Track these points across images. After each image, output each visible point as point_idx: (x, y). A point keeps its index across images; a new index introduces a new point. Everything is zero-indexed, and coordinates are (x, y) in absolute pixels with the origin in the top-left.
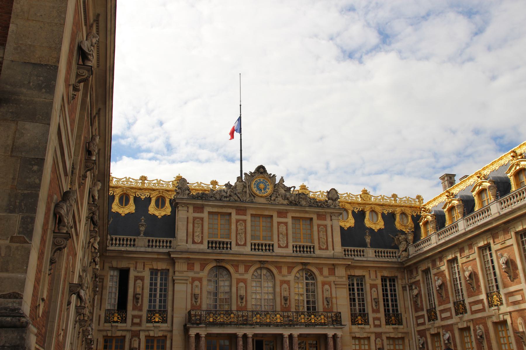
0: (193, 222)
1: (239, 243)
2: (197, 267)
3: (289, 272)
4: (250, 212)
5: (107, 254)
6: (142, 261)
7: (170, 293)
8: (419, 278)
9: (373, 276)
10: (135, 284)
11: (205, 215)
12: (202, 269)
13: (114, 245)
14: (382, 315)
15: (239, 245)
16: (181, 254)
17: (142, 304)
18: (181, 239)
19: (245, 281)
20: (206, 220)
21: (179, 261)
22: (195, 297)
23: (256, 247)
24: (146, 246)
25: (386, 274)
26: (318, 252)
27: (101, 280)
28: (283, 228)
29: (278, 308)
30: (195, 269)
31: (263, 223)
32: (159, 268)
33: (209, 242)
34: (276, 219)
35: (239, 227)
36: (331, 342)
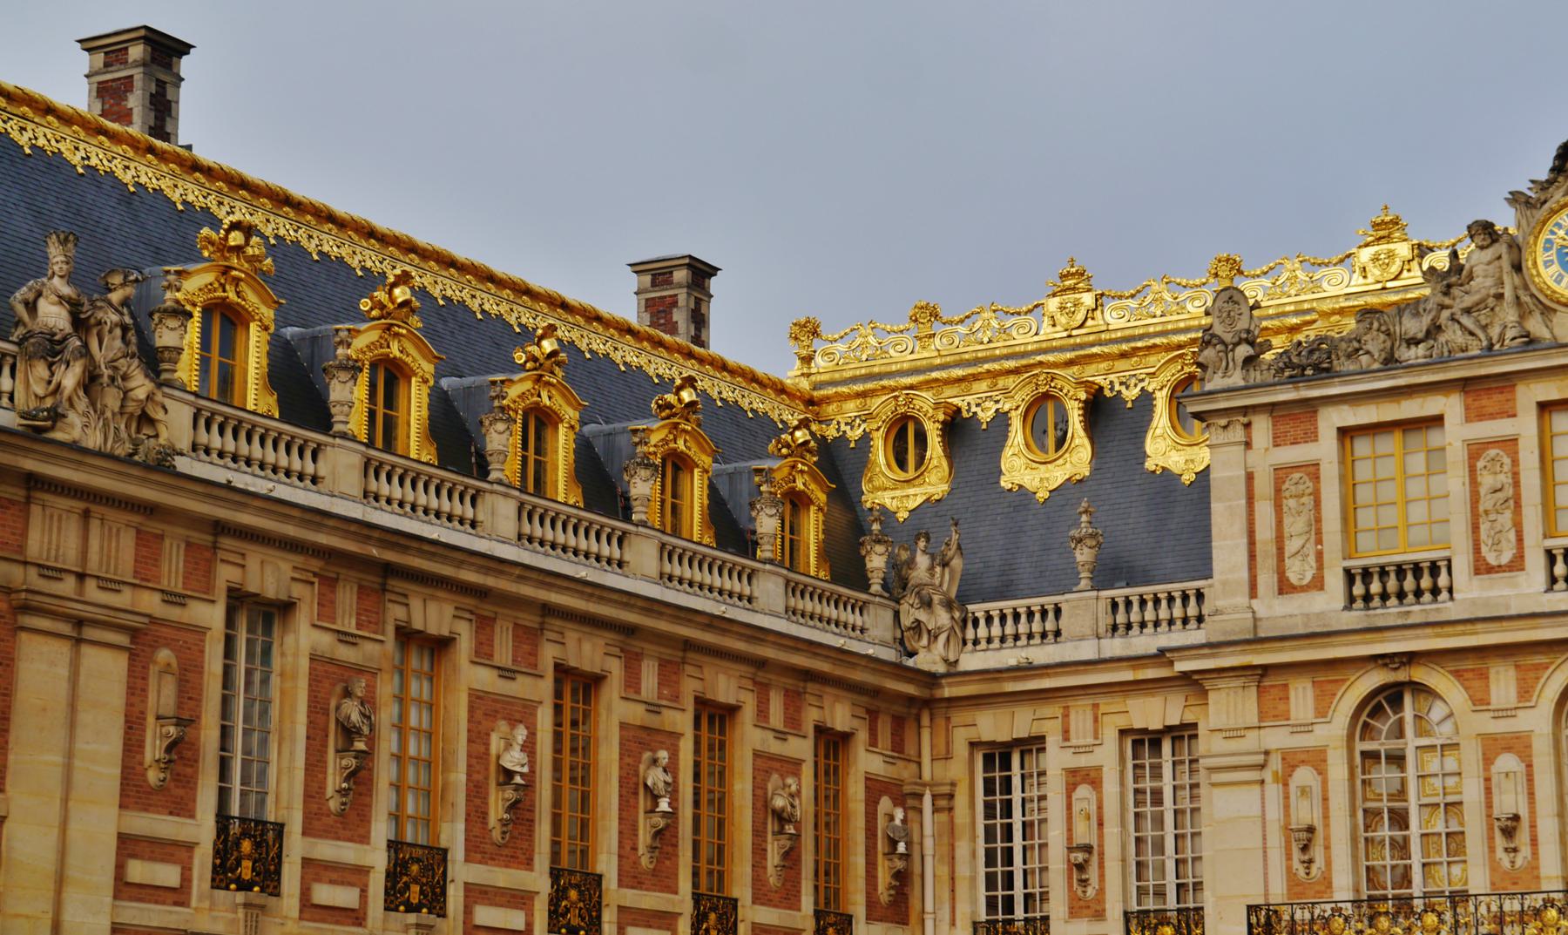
0: (1278, 491)
1: (1492, 561)
4: (1530, 394)
5: (947, 692)
6: (1090, 701)
10: (1069, 807)
13: (983, 645)
15: (1490, 570)
16: (1213, 656)
17: (1101, 891)
18: (1224, 583)
21: (1222, 684)
22: (1305, 840)
24: (1102, 630)
27: (943, 803)
30: (1293, 714)
32: (1156, 725)
33: (1349, 576)
35: (1487, 481)
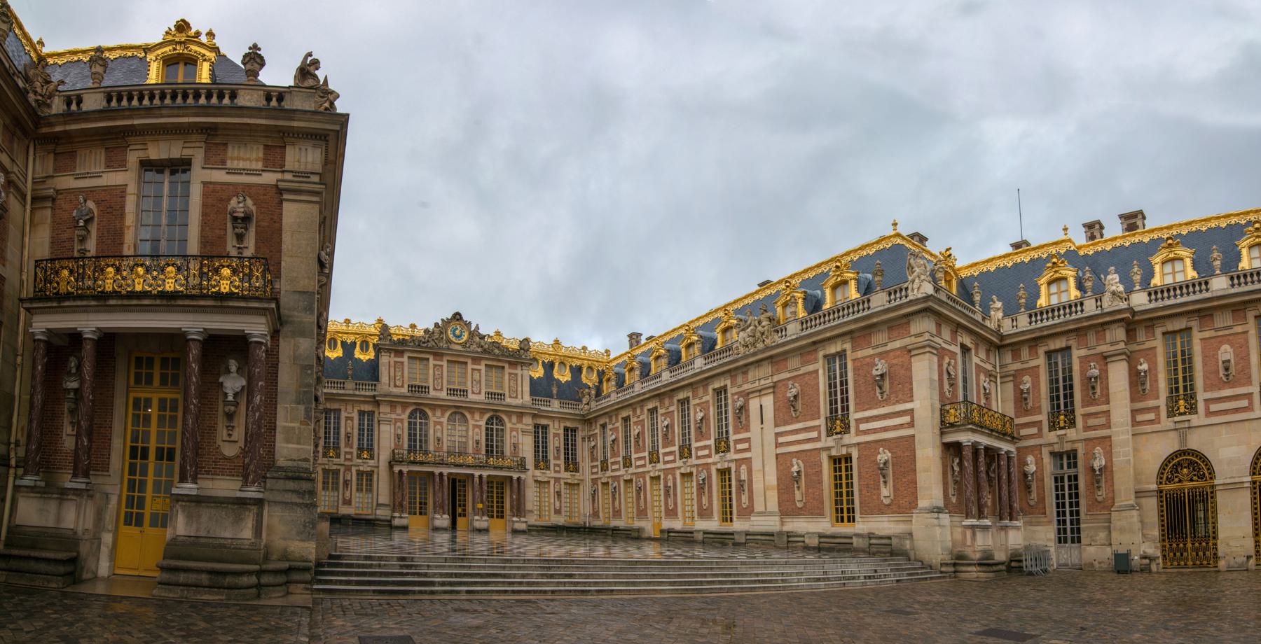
2: (399, 410)
3: (481, 418)
4: (445, 358)
7: (376, 433)
8: (597, 431)
9: (557, 426)
11: (405, 359)
12: (403, 412)
14: (561, 462)
19: (441, 423)
20: (406, 364)
22: (398, 437)
23: (452, 391)
25: (569, 424)
26: (508, 400)
28: (476, 376)
29: (470, 450)
31: (457, 369)
34: (470, 366)
36: (515, 485)
